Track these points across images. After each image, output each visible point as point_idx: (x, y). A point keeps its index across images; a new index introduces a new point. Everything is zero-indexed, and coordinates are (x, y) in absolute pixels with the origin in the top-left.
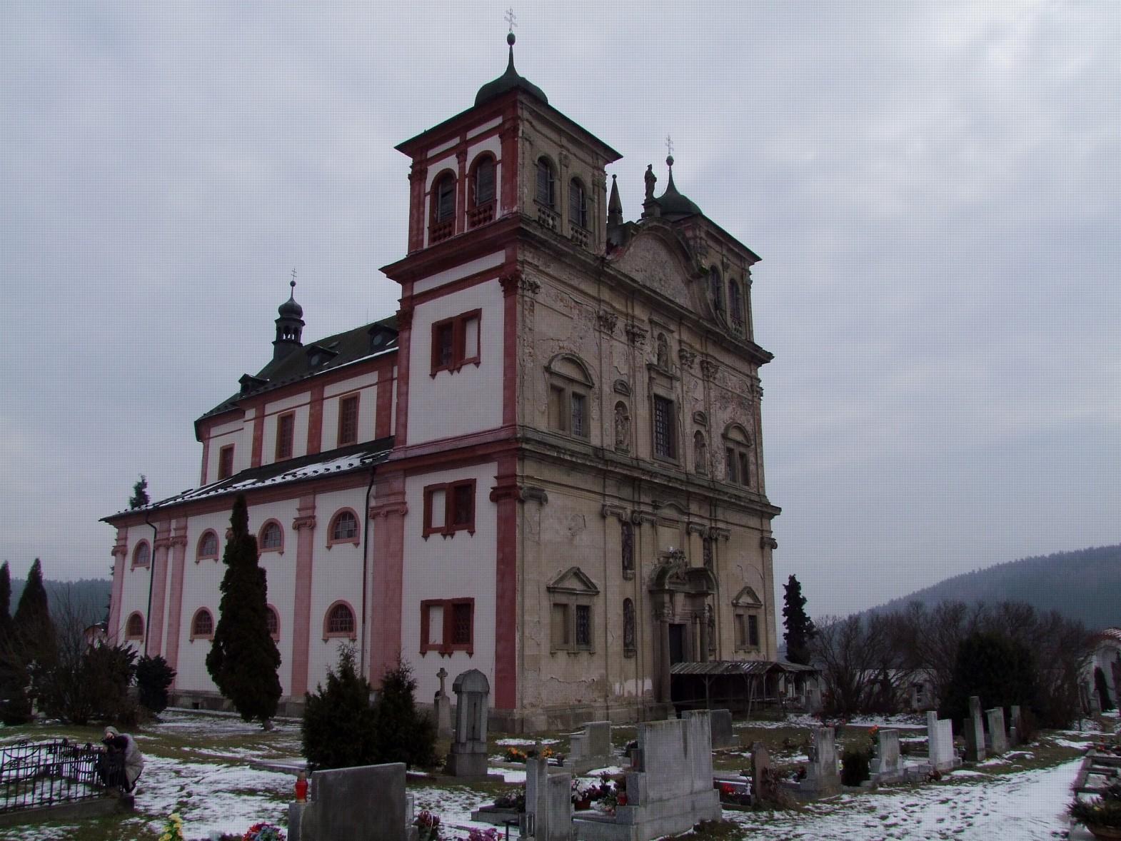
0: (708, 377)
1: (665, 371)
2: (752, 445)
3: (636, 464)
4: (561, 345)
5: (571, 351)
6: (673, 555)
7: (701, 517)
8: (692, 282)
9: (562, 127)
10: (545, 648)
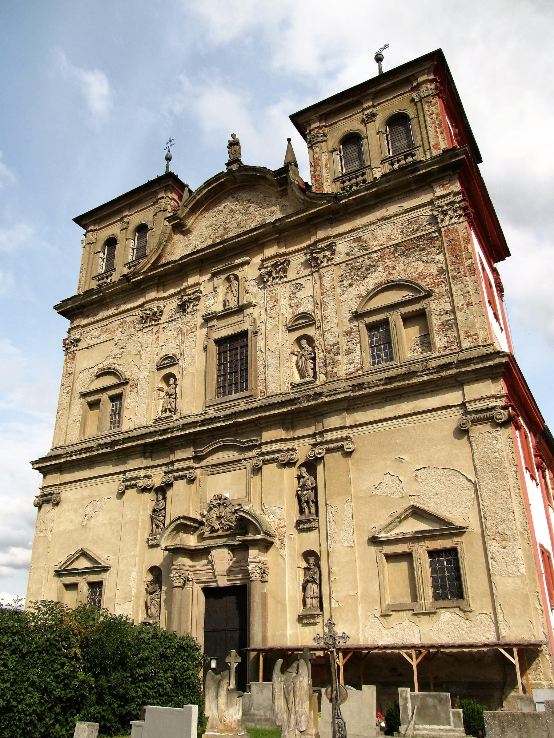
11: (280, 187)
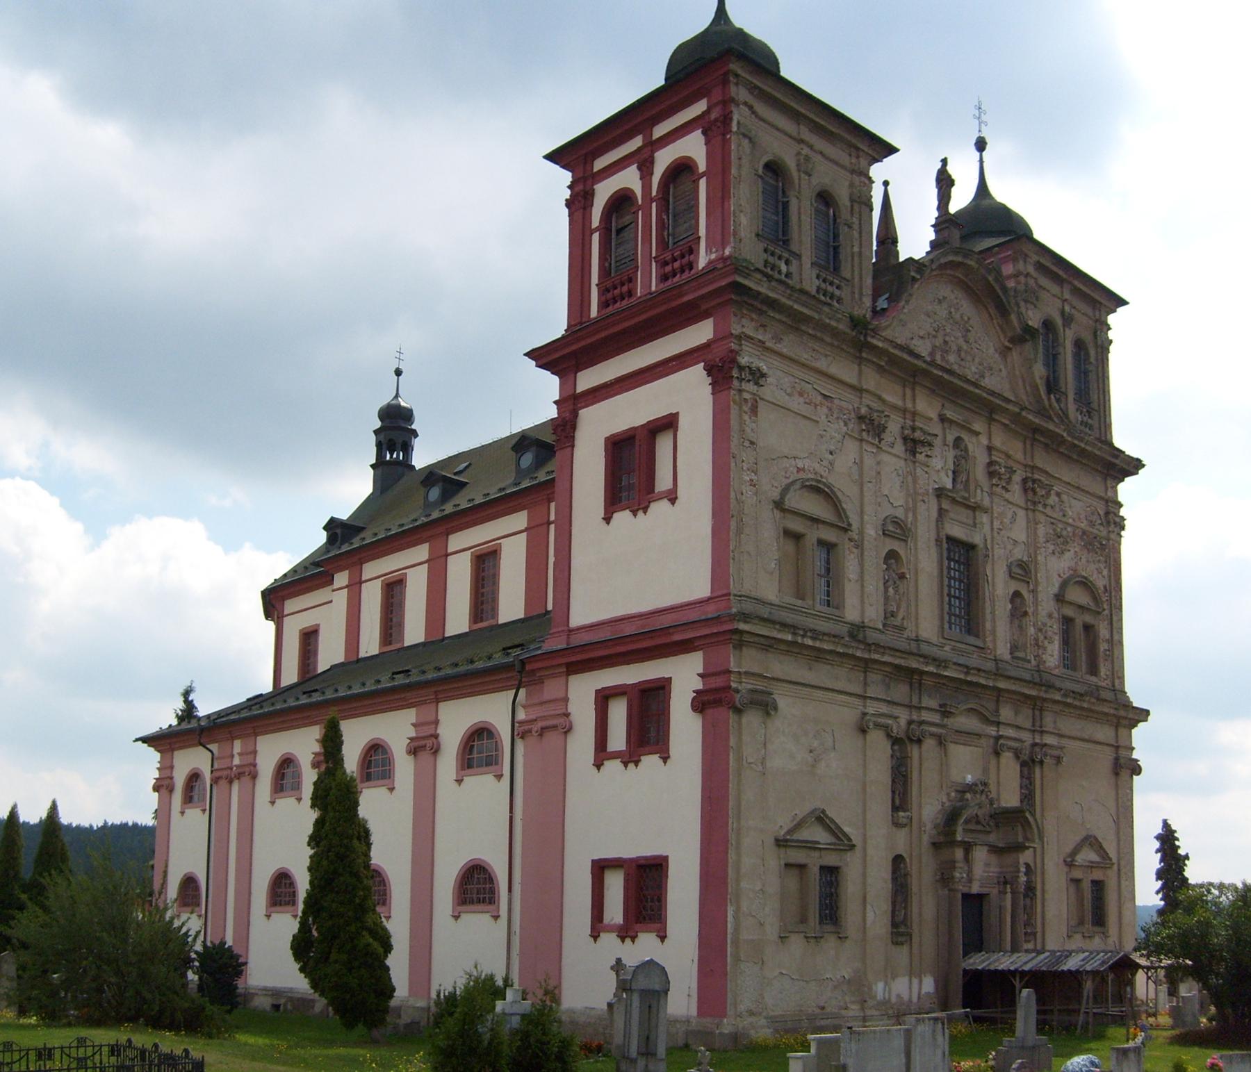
0: (1034, 503)
1: (965, 498)
2: (1104, 610)
3: (917, 648)
4: (800, 465)
5: (816, 473)
6: (970, 788)
7: (1018, 727)
8: (1010, 349)
9: (803, 111)
10: (772, 932)
11: (1009, 341)
